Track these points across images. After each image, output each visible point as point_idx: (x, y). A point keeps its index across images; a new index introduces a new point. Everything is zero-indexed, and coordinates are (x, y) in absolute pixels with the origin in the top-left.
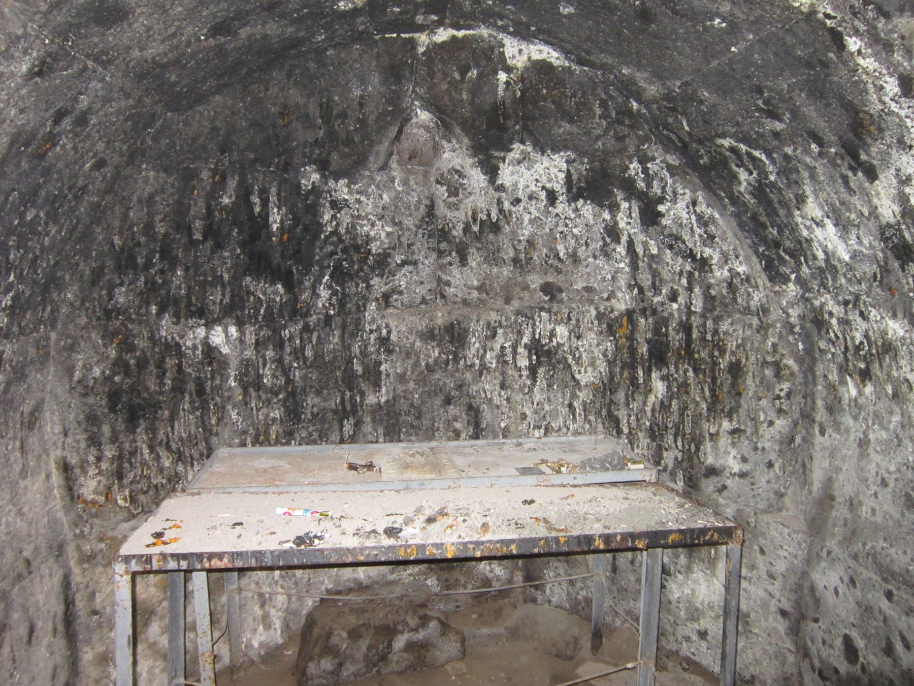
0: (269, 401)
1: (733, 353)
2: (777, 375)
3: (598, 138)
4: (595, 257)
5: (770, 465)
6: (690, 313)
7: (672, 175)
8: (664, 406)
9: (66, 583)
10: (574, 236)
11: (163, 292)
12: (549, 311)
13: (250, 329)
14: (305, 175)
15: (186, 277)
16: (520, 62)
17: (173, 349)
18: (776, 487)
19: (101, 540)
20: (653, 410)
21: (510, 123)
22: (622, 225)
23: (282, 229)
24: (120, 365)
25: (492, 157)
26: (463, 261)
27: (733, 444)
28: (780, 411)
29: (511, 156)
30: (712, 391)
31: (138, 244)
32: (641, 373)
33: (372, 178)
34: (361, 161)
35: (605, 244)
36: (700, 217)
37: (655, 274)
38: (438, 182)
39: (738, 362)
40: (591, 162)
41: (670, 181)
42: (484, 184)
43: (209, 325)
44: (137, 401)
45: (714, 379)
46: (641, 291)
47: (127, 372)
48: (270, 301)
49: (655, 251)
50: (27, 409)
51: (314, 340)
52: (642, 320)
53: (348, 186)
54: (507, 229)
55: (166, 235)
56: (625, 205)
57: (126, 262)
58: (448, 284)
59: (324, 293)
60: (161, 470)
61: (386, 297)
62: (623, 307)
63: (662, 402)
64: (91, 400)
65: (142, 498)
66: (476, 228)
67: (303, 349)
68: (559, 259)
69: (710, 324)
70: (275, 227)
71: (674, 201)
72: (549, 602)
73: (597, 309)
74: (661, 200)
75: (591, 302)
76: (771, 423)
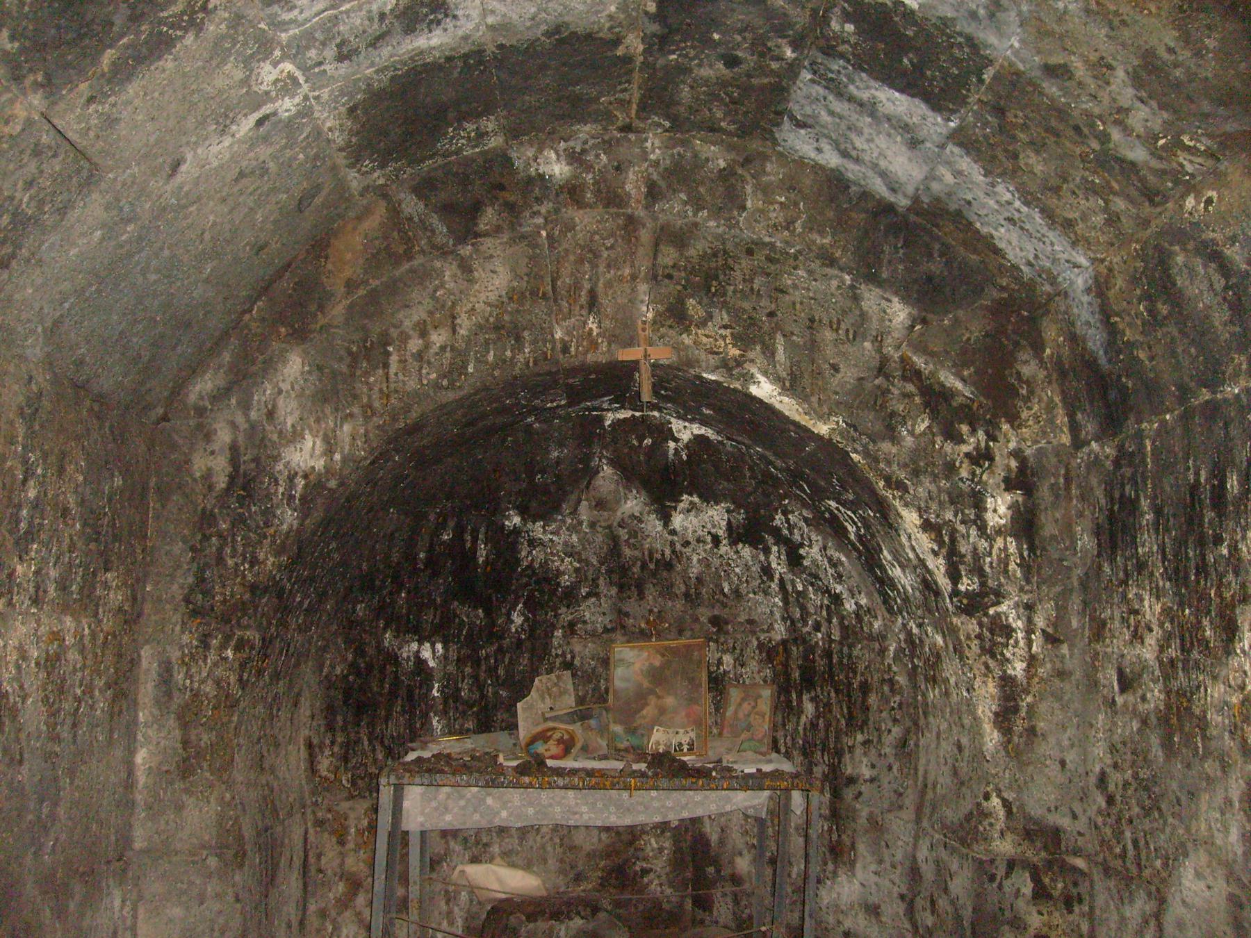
0: (464, 713)
1: (863, 674)
2: (892, 690)
3: (750, 494)
4: (755, 593)
5: (890, 768)
6: (831, 641)
7: (808, 525)
8: (814, 725)
9: (306, 840)
10: (737, 574)
11: (390, 610)
12: (717, 641)
13: (453, 648)
14: (508, 518)
15: (407, 600)
16: (685, 437)
17: (394, 658)
18: (895, 786)
19: (329, 810)
20: (805, 729)
21: (679, 479)
22: (774, 565)
23: (486, 562)
24: (353, 666)
25: (664, 506)
26: (641, 596)
27: (865, 754)
28: (895, 721)
29: (682, 505)
30: (849, 708)
31: (378, 570)
32: (794, 696)
33: (564, 522)
34: (557, 508)
35: (763, 582)
36: (830, 560)
37: (803, 608)
38: (620, 526)
39: (866, 680)
40: (746, 513)
41: (806, 530)
42: (660, 528)
43: (420, 642)
44: (363, 698)
45: (849, 696)
46: (793, 622)
47: (358, 674)
48: (471, 624)
49: (800, 588)
50: (296, 690)
51: (507, 661)
52: (794, 649)
53: (543, 527)
54: (679, 567)
55: (398, 563)
56: (775, 549)
57: (368, 584)
58: (627, 615)
59: (518, 619)
60: (375, 761)
61: (572, 625)
62: (778, 638)
63: (812, 723)
64: (332, 693)
65: (360, 782)
66: (652, 566)
67: (496, 668)
68: (725, 595)
69: (845, 649)
70: (481, 560)
71: (810, 546)
72: (717, 922)
73: (758, 639)
74: (802, 545)
75: (753, 633)
76: (890, 731)
